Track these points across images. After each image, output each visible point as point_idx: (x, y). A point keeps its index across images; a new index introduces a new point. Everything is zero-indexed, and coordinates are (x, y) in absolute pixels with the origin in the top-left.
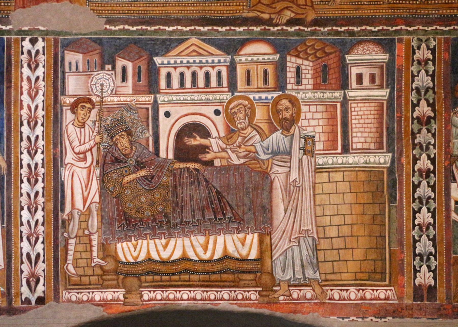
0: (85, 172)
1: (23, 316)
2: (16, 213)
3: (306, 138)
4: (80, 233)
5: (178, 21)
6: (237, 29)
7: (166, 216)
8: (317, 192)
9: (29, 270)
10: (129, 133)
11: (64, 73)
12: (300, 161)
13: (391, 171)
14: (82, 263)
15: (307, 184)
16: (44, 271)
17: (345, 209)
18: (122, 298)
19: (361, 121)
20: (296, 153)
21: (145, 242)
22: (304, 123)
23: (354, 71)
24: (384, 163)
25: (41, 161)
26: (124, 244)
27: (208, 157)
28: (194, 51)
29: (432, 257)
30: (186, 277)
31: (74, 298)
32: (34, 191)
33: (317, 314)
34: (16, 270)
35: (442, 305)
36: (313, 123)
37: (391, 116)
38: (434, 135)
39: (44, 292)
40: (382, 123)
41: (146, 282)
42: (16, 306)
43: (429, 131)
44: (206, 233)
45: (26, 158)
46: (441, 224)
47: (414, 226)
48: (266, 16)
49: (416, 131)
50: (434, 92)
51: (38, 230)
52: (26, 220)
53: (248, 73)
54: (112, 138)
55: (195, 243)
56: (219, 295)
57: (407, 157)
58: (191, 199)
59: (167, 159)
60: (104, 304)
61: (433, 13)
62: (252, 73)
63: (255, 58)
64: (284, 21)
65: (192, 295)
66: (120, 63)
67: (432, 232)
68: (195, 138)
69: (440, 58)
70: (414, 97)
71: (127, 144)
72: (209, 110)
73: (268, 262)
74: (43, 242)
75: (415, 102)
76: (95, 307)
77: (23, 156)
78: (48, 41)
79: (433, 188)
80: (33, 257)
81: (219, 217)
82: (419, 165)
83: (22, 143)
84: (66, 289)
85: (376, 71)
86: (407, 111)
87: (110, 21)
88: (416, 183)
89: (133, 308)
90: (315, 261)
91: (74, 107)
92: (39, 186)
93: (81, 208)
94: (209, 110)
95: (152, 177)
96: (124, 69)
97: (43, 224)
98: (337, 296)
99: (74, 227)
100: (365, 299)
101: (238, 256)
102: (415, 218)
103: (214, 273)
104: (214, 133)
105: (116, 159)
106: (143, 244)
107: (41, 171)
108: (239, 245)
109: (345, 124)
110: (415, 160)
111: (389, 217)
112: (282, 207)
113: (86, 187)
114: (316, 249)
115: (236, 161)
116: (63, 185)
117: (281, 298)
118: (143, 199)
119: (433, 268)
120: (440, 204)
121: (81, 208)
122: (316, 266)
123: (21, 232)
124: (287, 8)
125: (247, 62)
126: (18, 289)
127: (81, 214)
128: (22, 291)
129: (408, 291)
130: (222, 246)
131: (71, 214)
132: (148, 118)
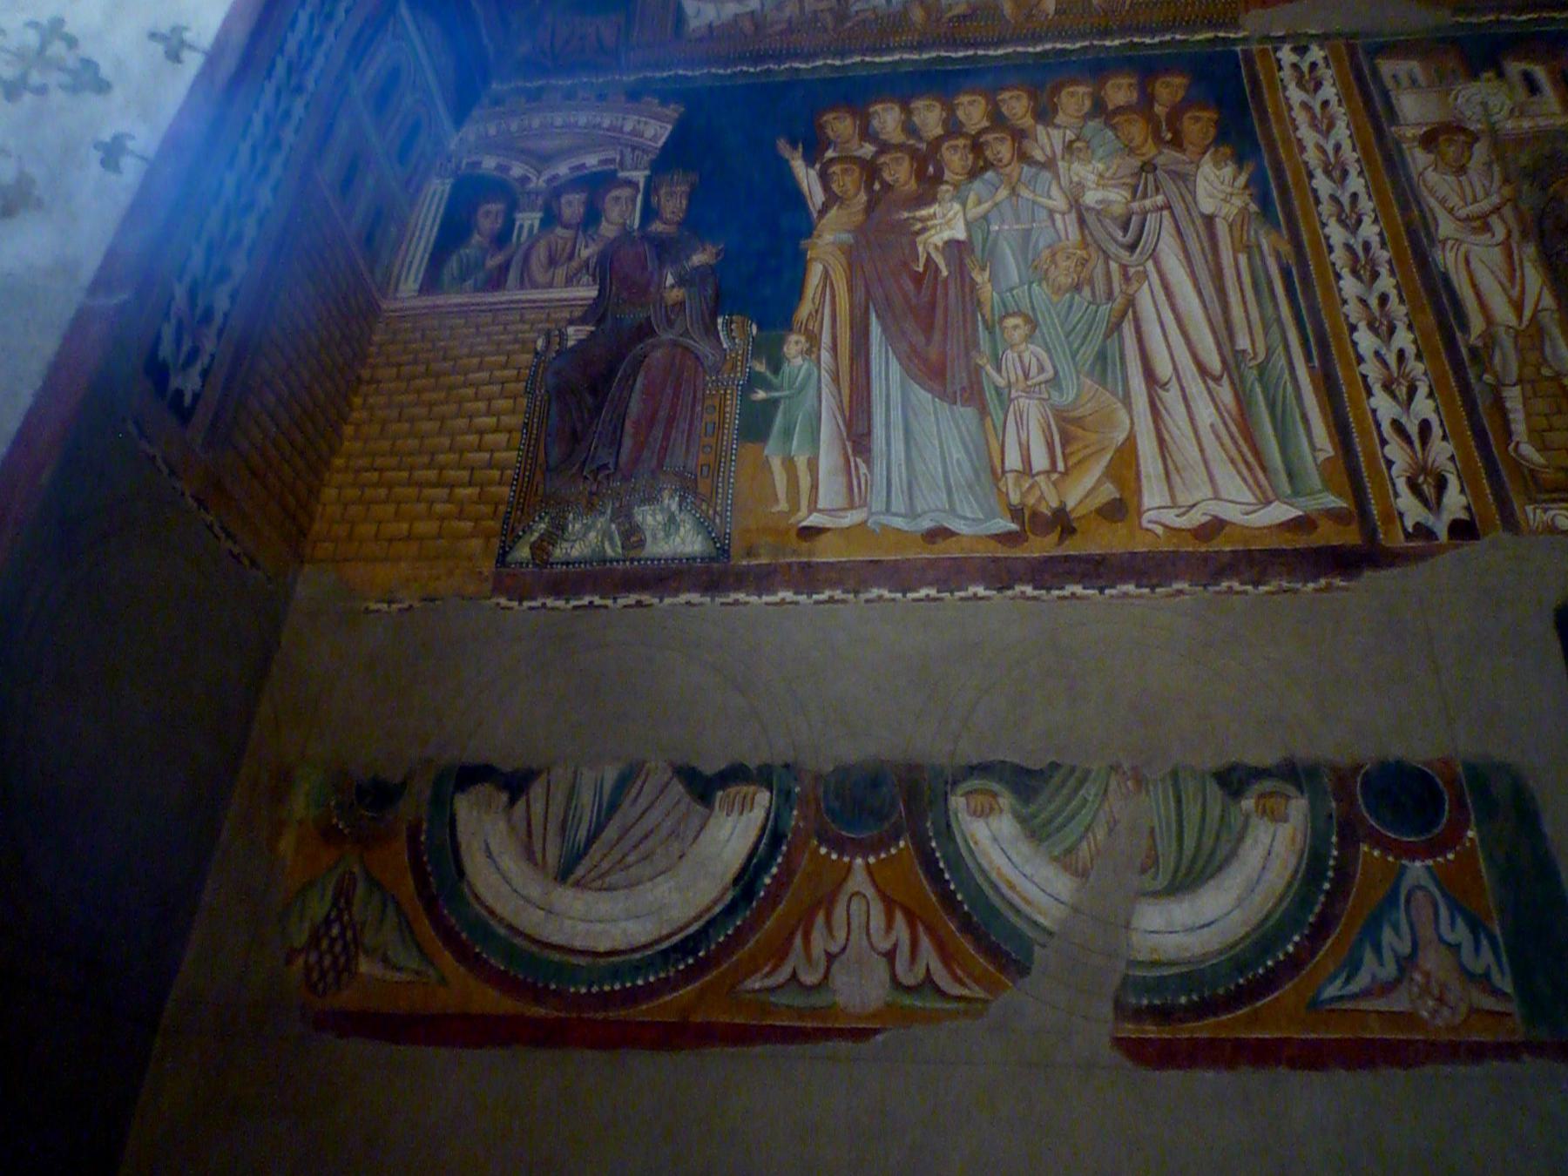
0: (1497, 255)
2: (1338, 337)
4: (1529, 372)
9: (1408, 460)
16: (1452, 458)
25: (1377, 239)
32: (1376, 294)
34: (1372, 458)
39: (1468, 508)
42: (1388, 545)
45: (1336, 234)
51: (1407, 370)
52: (1372, 350)
54: (1544, 188)
74: (1431, 395)
80: (1413, 430)
83: (1321, 208)
84: (1532, 501)
91: (1429, 140)
97: (1419, 357)
99: (1507, 360)
113: (1512, 278)
116: (1446, 278)
121: (1513, 322)
123: (1364, 377)
131: (1490, 338)
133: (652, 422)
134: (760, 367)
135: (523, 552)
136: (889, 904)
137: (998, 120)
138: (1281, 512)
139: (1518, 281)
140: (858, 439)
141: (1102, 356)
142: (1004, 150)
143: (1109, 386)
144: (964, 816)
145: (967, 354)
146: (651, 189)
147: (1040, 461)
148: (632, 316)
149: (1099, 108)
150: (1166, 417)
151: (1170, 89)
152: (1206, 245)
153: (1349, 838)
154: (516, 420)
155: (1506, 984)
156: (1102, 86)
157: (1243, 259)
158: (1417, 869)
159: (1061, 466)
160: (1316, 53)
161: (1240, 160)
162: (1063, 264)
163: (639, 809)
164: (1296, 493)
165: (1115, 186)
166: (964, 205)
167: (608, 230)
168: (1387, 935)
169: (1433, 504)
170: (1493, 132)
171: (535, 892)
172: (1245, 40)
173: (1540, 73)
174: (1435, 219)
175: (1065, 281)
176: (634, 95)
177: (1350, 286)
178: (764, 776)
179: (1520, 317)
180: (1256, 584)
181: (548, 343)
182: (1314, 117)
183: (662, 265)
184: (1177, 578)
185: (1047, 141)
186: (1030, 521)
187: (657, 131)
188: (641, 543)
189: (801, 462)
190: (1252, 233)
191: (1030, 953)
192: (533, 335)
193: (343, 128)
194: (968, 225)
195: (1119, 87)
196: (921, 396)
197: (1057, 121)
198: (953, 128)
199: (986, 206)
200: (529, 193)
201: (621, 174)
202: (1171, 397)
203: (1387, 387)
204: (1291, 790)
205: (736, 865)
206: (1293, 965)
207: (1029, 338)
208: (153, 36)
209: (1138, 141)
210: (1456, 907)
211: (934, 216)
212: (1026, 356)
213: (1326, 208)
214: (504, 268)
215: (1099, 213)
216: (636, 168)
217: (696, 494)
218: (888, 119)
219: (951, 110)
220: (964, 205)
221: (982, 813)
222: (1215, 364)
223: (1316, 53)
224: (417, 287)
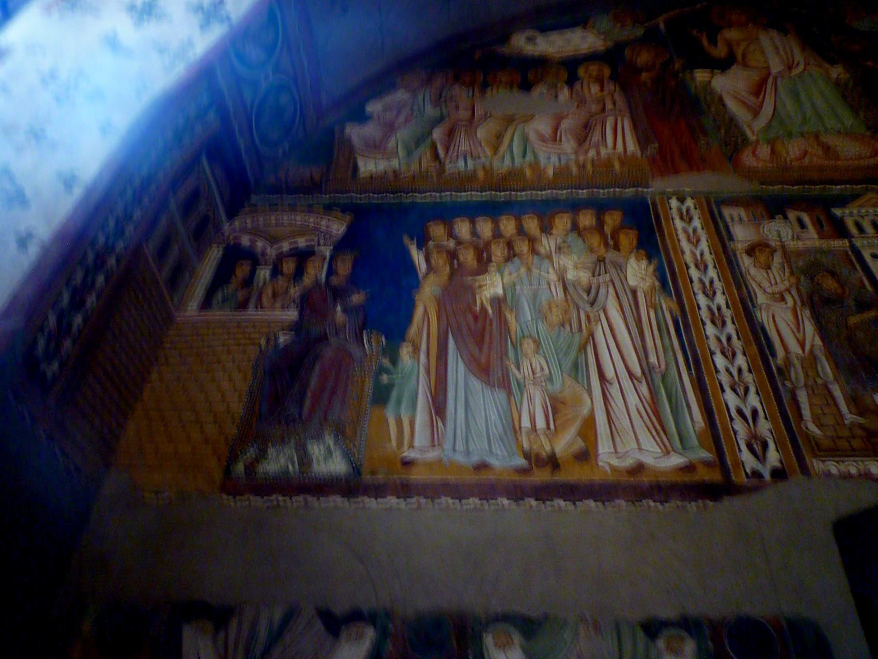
10: (833, 274)
14: (829, 421)
34: (726, 429)
45: (702, 300)
71: (836, 285)
80: (748, 413)
84: (815, 456)
99: (797, 374)
113: (799, 331)
116: (763, 329)
121: (800, 352)
127: (802, 361)
128: (743, 459)
131: (787, 359)
132: (851, 261)
135: (240, 468)
137: (521, 231)
138: (676, 460)
139: (802, 330)
140: (438, 407)
141: (576, 366)
142: (523, 247)
143: (580, 380)
145: (502, 359)
147: (541, 423)
150: (610, 399)
151: (612, 220)
152: (632, 302)
159: (552, 426)
160: (689, 203)
161: (650, 259)
162: (554, 310)
164: (684, 448)
167: (307, 281)
169: (761, 457)
170: (783, 247)
173: (806, 218)
174: (756, 294)
176: (328, 208)
177: (710, 330)
178: (372, 618)
179: (803, 349)
185: (547, 244)
186: (535, 460)
187: (338, 227)
190: (657, 298)
193: (164, 220)
196: (476, 384)
198: (497, 234)
202: (614, 390)
203: (734, 390)
204: (684, 634)
207: (537, 352)
213: (697, 286)
218: (463, 228)
222: (637, 371)
223: (689, 203)
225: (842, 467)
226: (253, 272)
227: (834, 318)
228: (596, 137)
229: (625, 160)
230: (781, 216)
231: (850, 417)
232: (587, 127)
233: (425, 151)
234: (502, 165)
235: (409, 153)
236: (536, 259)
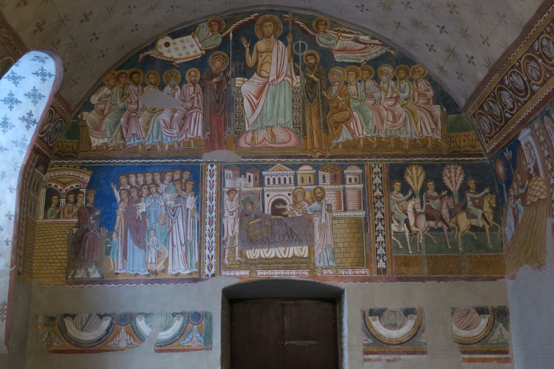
0: (233, 220)
1: (205, 282)
2: (203, 238)
3: (328, 205)
4: (231, 246)
5: (272, 157)
6: (297, 160)
7: (268, 239)
8: (333, 228)
10: (252, 203)
11: (224, 179)
12: (326, 214)
13: (365, 219)
14: (231, 259)
15: (329, 225)
17: (346, 235)
18: (248, 274)
19: (352, 198)
20: (324, 212)
21: (258, 250)
22: (327, 199)
23: (348, 177)
24: (363, 215)
26: (250, 251)
27: (286, 213)
28: (279, 169)
29: (384, 256)
30: (276, 265)
31: (227, 275)
33: (334, 281)
35: (389, 277)
36: (331, 198)
37: (364, 196)
38: (383, 204)
40: (361, 199)
41: (259, 267)
43: (381, 202)
44: (285, 246)
45: (208, 214)
46: (388, 242)
47: (376, 242)
48: (309, 155)
49: (375, 202)
50: (382, 186)
53: (302, 178)
55: (280, 250)
56: (291, 273)
57: (372, 213)
58: (279, 231)
59: (268, 214)
60: (241, 277)
61: (380, 153)
62: (304, 178)
63: (305, 172)
64: (317, 156)
65: (279, 273)
66: (248, 174)
67: (384, 245)
68: (280, 205)
69: (384, 171)
70: (374, 188)
71: (251, 208)
72: (286, 194)
73: (313, 259)
75: (374, 190)
76: (236, 278)
77: (207, 214)
78: (218, 165)
79: (384, 226)
81: (291, 239)
82: (377, 216)
85: (357, 177)
86: (371, 194)
87: (243, 157)
88: (376, 224)
89: (253, 279)
90: (333, 258)
92: (214, 226)
93: (231, 235)
94: (286, 194)
95: (262, 222)
96: (250, 177)
97: (215, 243)
98: (343, 273)
99: (228, 244)
100: (356, 274)
101: (299, 256)
102: (376, 239)
103: (289, 263)
104: (288, 203)
105: (246, 214)
106: (258, 251)
107: (215, 220)
108: (300, 251)
109: (345, 199)
110: (376, 214)
111: (365, 239)
112: (318, 234)
113: (233, 226)
114: (334, 253)
115: (298, 215)
117: (319, 274)
118: (258, 232)
119: (385, 261)
120: (387, 233)
121: (231, 235)
122: (334, 260)
124: (318, 151)
125: (302, 174)
126: (203, 270)
127: (231, 238)
129: (375, 271)
130: (292, 252)
131: (227, 238)
132: (260, 197)
133: (90, 251)
134: (109, 240)
135: (70, 277)
136: (127, 333)
137: (153, 180)
138: (188, 272)
140: (125, 256)
141: (166, 240)
144: (138, 321)
146: (87, 195)
147: (154, 261)
148: (85, 227)
149: (173, 180)
151: (186, 175)
153: (187, 323)
154: (66, 249)
155: (203, 342)
156: (173, 173)
157: (192, 219)
158: (195, 327)
163: (92, 320)
164: (191, 268)
165: (173, 200)
166: (146, 203)
167: (79, 204)
168: (190, 336)
170: (240, 191)
171: (78, 333)
172: (202, 162)
173: (252, 176)
175: (162, 223)
176: (82, 168)
178: (110, 315)
180: (182, 284)
181: (70, 233)
182: (210, 185)
183: (90, 215)
184: (171, 283)
187: (87, 178)
188: (89, 275)
189: (115, 260)
191: (145, 339)
192: (67, 230)
194: (146, 208)
195: (177, 173)
197: (165, 182)
199: (150, 203)
200: (62, 194)
201: (81, 190)
202: (175, 249)
204: (182, 316)
205: (106, 328)
206: (178, 339)
207: (154, 235)
208: (6, 215)
209: (178, 189)
210: (199, 332)
211: (140, 206)
212: (153, 239)
213: (208, 208)
214: (60, 213)
215: (169, 207)
216: (83, 188)
217: (98, 266)
218: (133, 179)
219: (145, 177)
220: (146, 203)
221: (140, 320)
222: (183, 242)
223: (215, 167)
224: (43, 217)
225: (230, 273)
226: (59, 202)
227: (245, 222)
228: (187, 127)
229: (196, 141)
230: (243, 176)
231: (237, 258)
232: (184, 118)
233: (117, 132)
234: (149, 143)
235: (112, 133)
236: (158, 195)
